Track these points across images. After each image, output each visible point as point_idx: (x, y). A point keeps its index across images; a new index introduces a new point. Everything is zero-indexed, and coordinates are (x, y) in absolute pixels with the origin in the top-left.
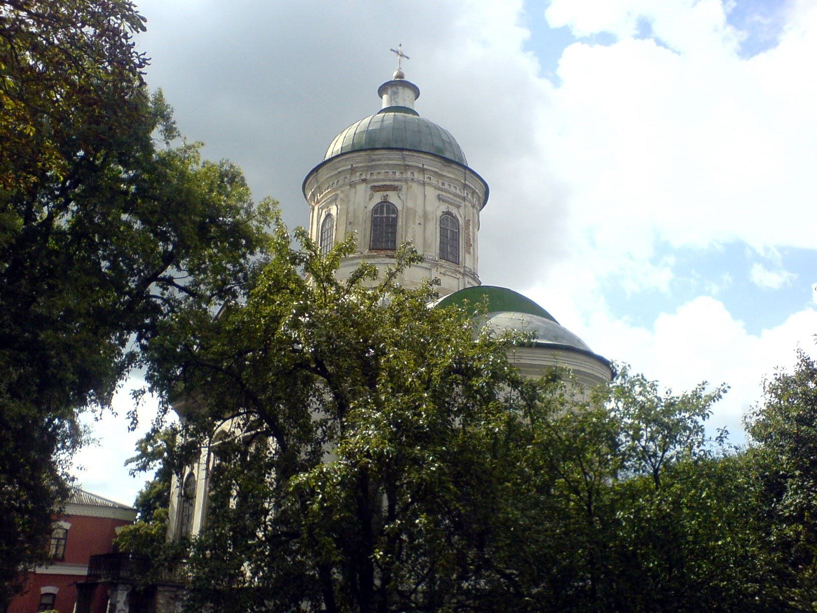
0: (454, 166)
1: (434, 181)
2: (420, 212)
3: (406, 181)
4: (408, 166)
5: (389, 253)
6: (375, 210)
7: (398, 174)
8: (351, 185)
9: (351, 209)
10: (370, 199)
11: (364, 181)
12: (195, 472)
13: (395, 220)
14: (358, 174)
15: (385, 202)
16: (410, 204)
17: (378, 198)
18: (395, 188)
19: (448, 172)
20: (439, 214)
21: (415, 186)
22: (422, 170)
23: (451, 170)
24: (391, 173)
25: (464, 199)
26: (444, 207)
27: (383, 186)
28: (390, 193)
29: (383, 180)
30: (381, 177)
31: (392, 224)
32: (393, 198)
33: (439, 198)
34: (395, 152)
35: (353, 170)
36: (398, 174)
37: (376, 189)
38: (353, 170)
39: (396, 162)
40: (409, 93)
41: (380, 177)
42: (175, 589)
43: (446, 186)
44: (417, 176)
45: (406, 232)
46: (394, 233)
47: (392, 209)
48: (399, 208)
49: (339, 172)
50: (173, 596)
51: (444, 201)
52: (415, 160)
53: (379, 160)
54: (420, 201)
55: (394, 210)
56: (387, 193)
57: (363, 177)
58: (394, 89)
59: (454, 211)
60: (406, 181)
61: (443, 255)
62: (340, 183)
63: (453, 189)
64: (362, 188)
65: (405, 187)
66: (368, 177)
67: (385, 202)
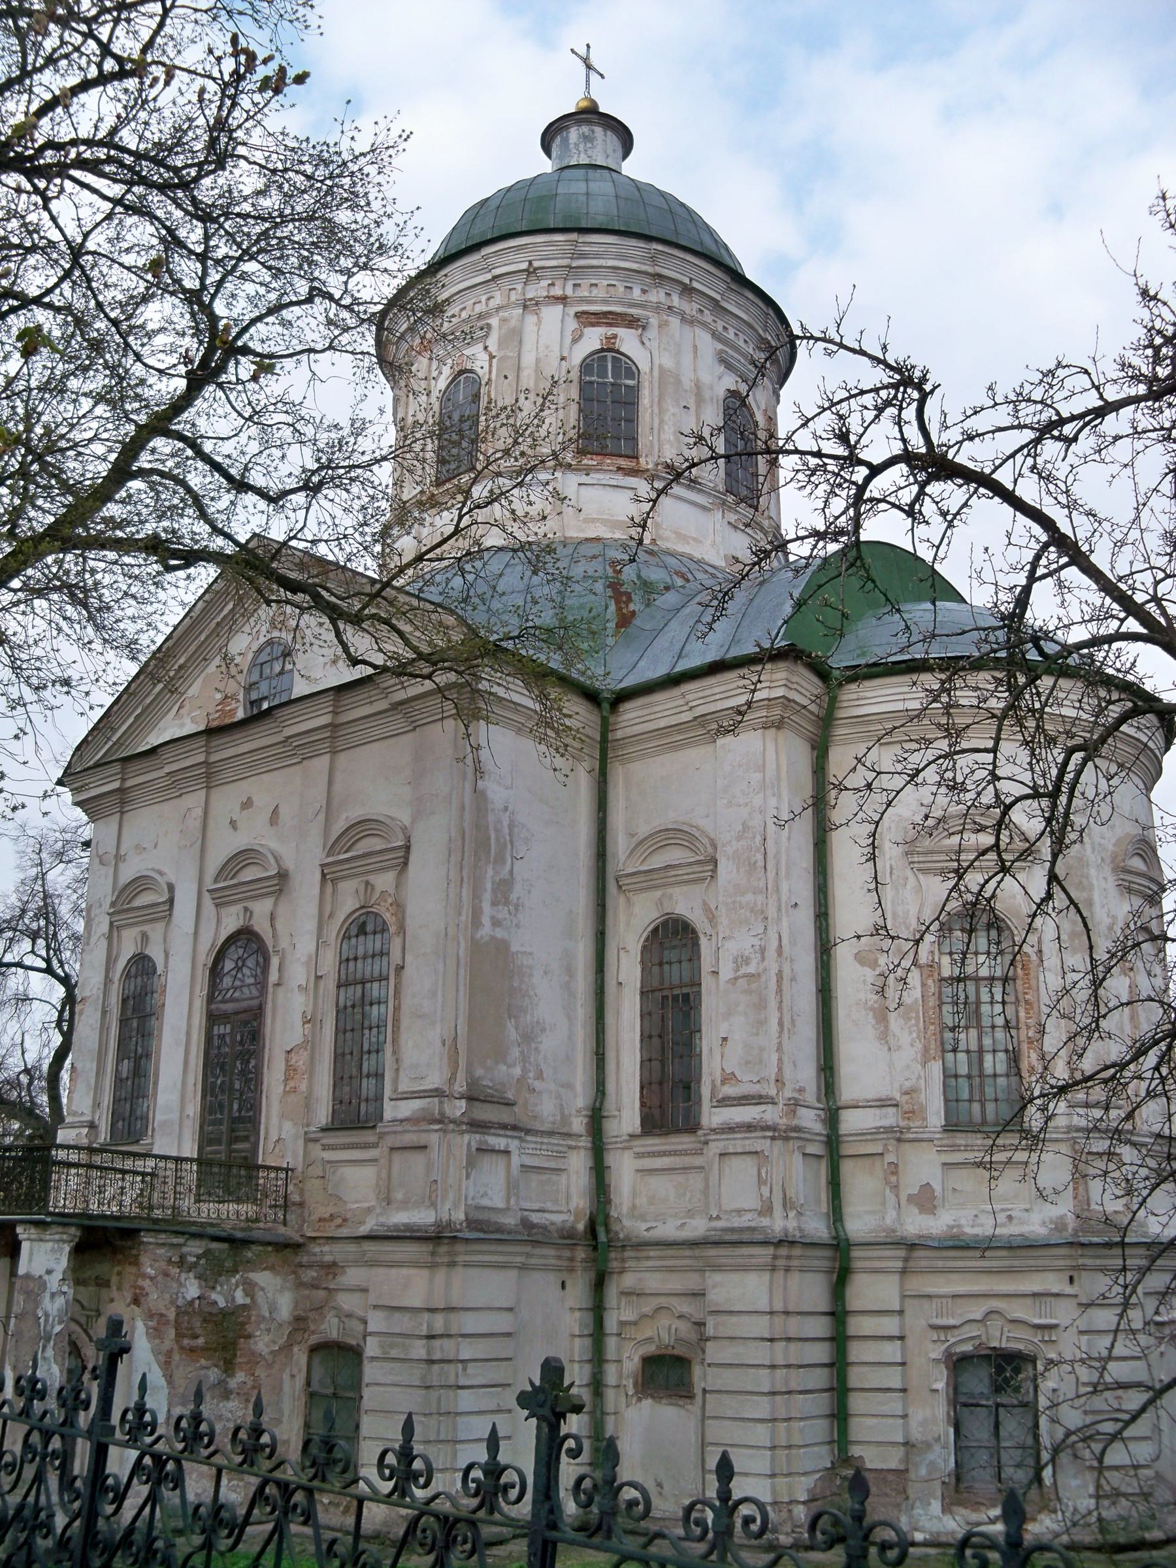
0: (750, 295)
1: (708, 317)
3: (657, 308)
4: (660, 276)
5: (623, 462)
6: (586, 366)
7: (637, 292)
8: (525, 307)
9: (528, 359)
10: (575, 341)
11: (563, 300)
12: (155, 952)
13: (634, 391)
14: (545, 283)
15: (609, 349)
16: (668, 362)
17: (593, 339)
18: (631, 322)
19: (739, 306)
20: (721, 393)
21: (675, 321)
22: (687, 291)
23: (742, 301)
24: (622, 289)
27: (606, 314)
28: (621, 332)
29: (605, 302)
31: (629, 401)
32: (628, 342)
33: (723, 360)
34: (633, 242)
35: (531, 272)
36: (637, 292)
37: (588, 319)
38: (531, 272)
39: (634, 266)
40: (612, 141)
41: (599, 293)
42: (181, 1240)
43: (731, 335)
44: (676, 300)
45: (662, 422)
46: (632, 420)
47: (625, 367)
48: (643, 365)
49: (495, 278)
50: (175, 1259)
51: (729, 366)
52: (678, 267)
53: (597, 256)
54: (687, 359)
55: (632, 371)
56: (615, 330)
57: (557, 291)
58: (585, 129)
60: (657, 308)
62: (492, 303)
64: (552, 314)
65: (654, 321)
66: (569, 291)
67: (609, 349)
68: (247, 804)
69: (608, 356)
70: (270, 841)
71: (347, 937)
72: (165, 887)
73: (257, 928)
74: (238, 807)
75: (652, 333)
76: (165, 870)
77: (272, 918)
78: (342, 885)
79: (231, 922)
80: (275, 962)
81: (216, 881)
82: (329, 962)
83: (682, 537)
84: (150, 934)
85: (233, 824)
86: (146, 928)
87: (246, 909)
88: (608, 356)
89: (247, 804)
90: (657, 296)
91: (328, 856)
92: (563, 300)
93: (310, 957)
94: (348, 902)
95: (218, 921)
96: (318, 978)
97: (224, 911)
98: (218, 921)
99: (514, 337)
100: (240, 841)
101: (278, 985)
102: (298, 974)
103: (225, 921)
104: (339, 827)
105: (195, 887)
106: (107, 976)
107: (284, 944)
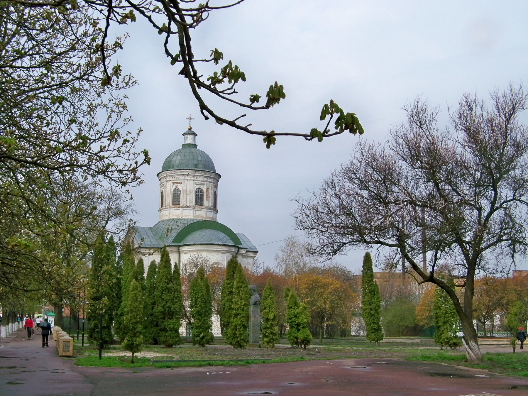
2: (188, 190)
5: (178, 206)
11: (171, 181)
15: (177, 188)
25: (205, 181)
26: (197, 187)
30: (175, 179)
31: (179, 196)
32: (179, 186)
37: (174, 183)
41: (175, 179)
59: (202, 187)
61: (197, 204)
63: (200, 179)
64: (170, 182)
67: (177, 188)
69: (176, 189)
75: (183, 184)
83: (186, 216)
88: (176, 189)
90: (183, 178)
92: (171, 181)
99: (166, 187)
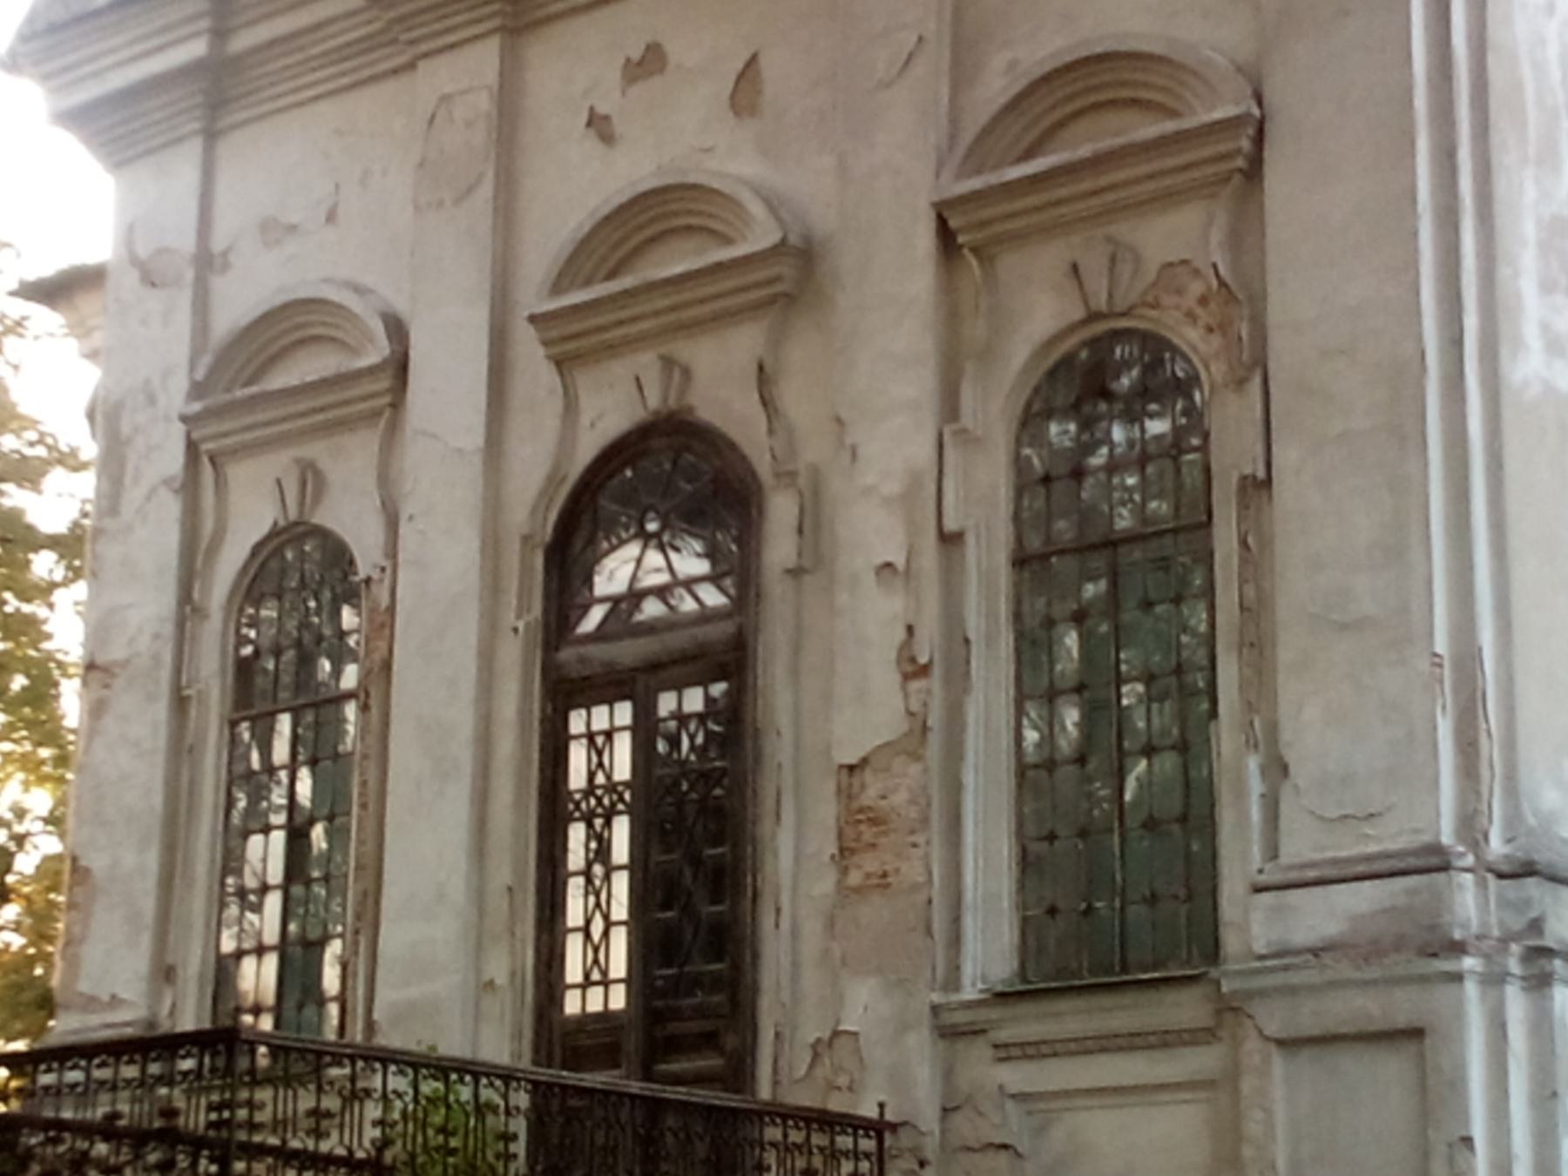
68: (648, 63)
70: (733, 161)
71: (1030, 421)
72: (378, 327)
73: (707, 412)
74: (614, 76)
76: (367, 280)
77: (764, 377)
78: (1010, 263)
79: (611, 407)
80: (781, 511)
81: (558, 286)
82: (985, 495)
84: (325, 464)
85: (598, 124)
86: (316, 450)
87: (668, 363)
89: (648, 63)
91: (961, 175)
93: (915, 482)
94: (1038, 310)
95: (570, 407)
96: (950, 540)
97: (584, 380)
98: (570, 407)
100: (631, 170)
101: (796, 573)
102: (872, 531)
103: (589, 405)
104: (995, 87)
105: (478, 318)
106: (185, 596)
107: (814, 450)
